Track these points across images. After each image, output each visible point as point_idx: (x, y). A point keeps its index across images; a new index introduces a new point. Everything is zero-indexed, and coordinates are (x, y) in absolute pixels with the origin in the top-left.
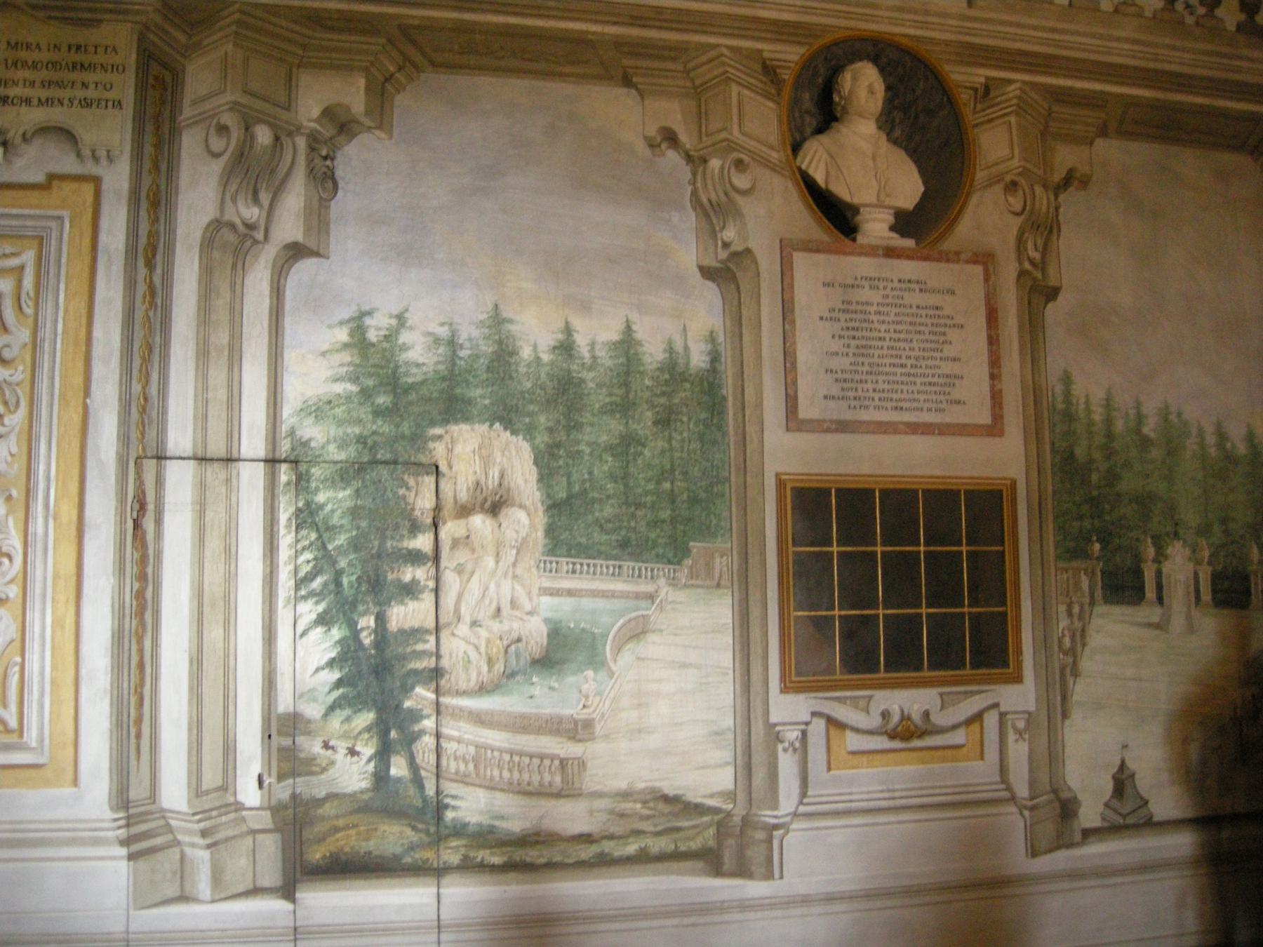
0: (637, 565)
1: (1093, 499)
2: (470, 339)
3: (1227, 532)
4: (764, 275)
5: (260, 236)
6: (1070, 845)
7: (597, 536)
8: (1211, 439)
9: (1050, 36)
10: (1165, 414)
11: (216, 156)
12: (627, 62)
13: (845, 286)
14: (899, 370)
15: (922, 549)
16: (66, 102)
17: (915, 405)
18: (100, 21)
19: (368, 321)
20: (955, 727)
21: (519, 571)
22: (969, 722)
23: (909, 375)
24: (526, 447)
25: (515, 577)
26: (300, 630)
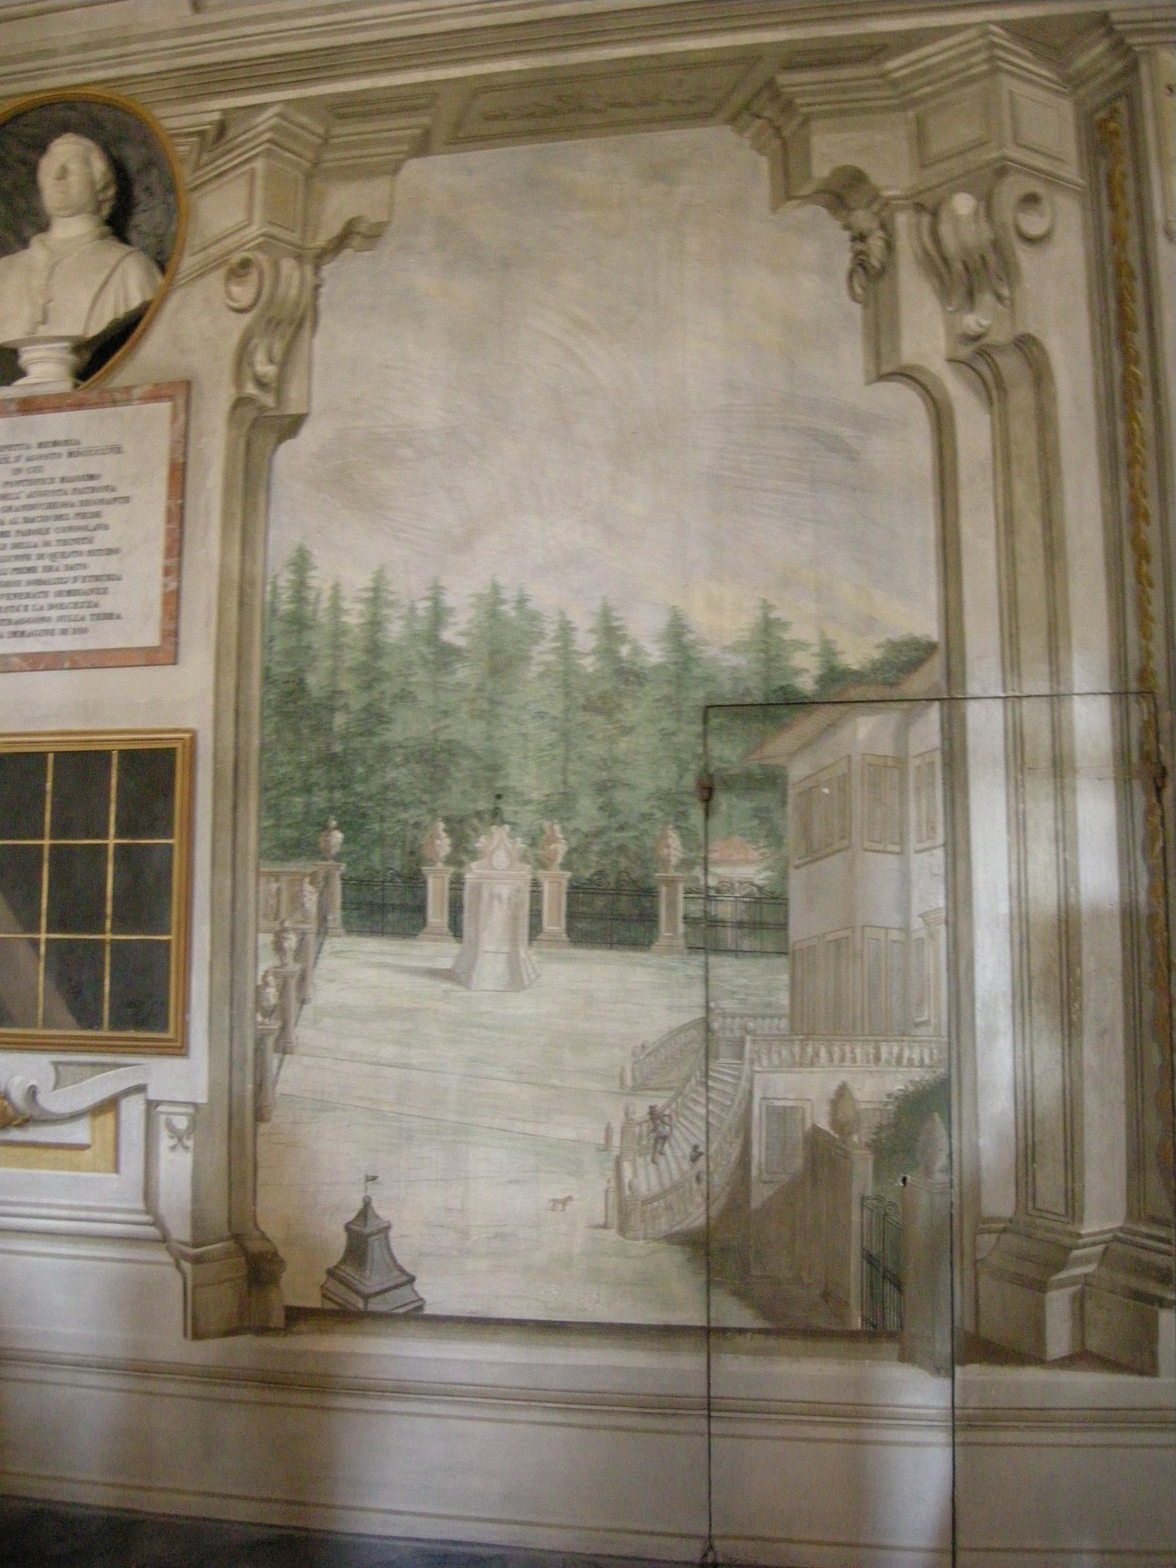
1: (333, 756)
3: (609, 809)
6: (263, 1330)
8: (586, 641)
10: (491, 603)
15: (47, 842)
20: (74, 1117)
23: (39, 582)
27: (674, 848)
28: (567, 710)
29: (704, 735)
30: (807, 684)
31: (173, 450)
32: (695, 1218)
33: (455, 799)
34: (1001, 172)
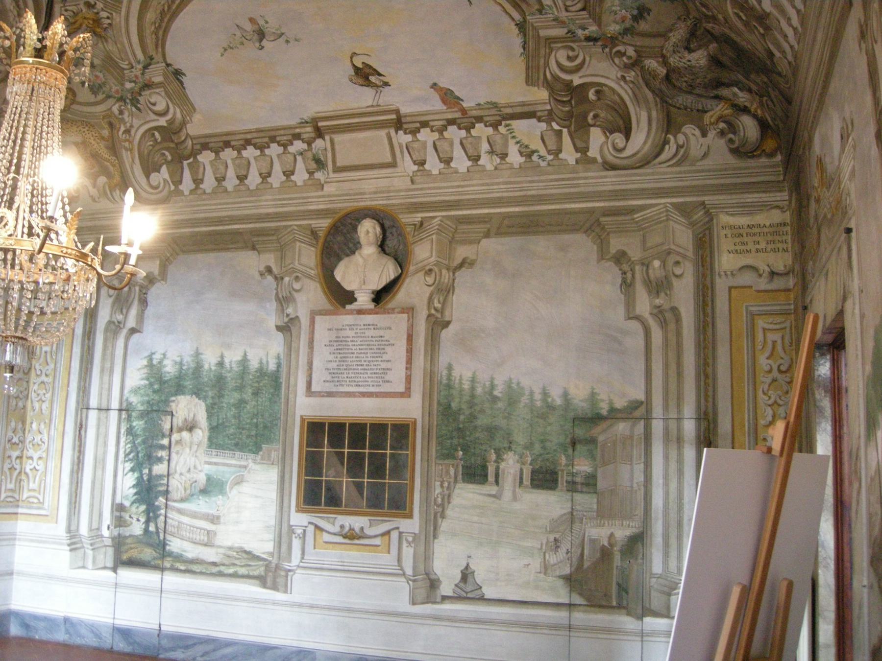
0: (241, 453)
2: (187, 362)
3: (544, 448)
4: (303, 327)
5: (122, 326)
6: (435, 603)
7: (227, 441)
8: (538, 396)
9: (457, 190)
10: (509, 384)
11: (110, 296)
12: (255, 239)
13: (337, 330)
14: (360, 367)
15: (367, 451)
17: (366, 383)
19: (154, 356)
20: (375, 536)
21: (198, 454)
22: (383, 535)
23: (365, 369)
24: (203, 404)
25: (196, 456)
26: (125, 472)
27: (563, 460)
28: (532, 417)
29: (574, 426)
30: (604, 412)
31: (408, 330)
32: (567, 571)
33: (497, 443)
34: (669, 253)
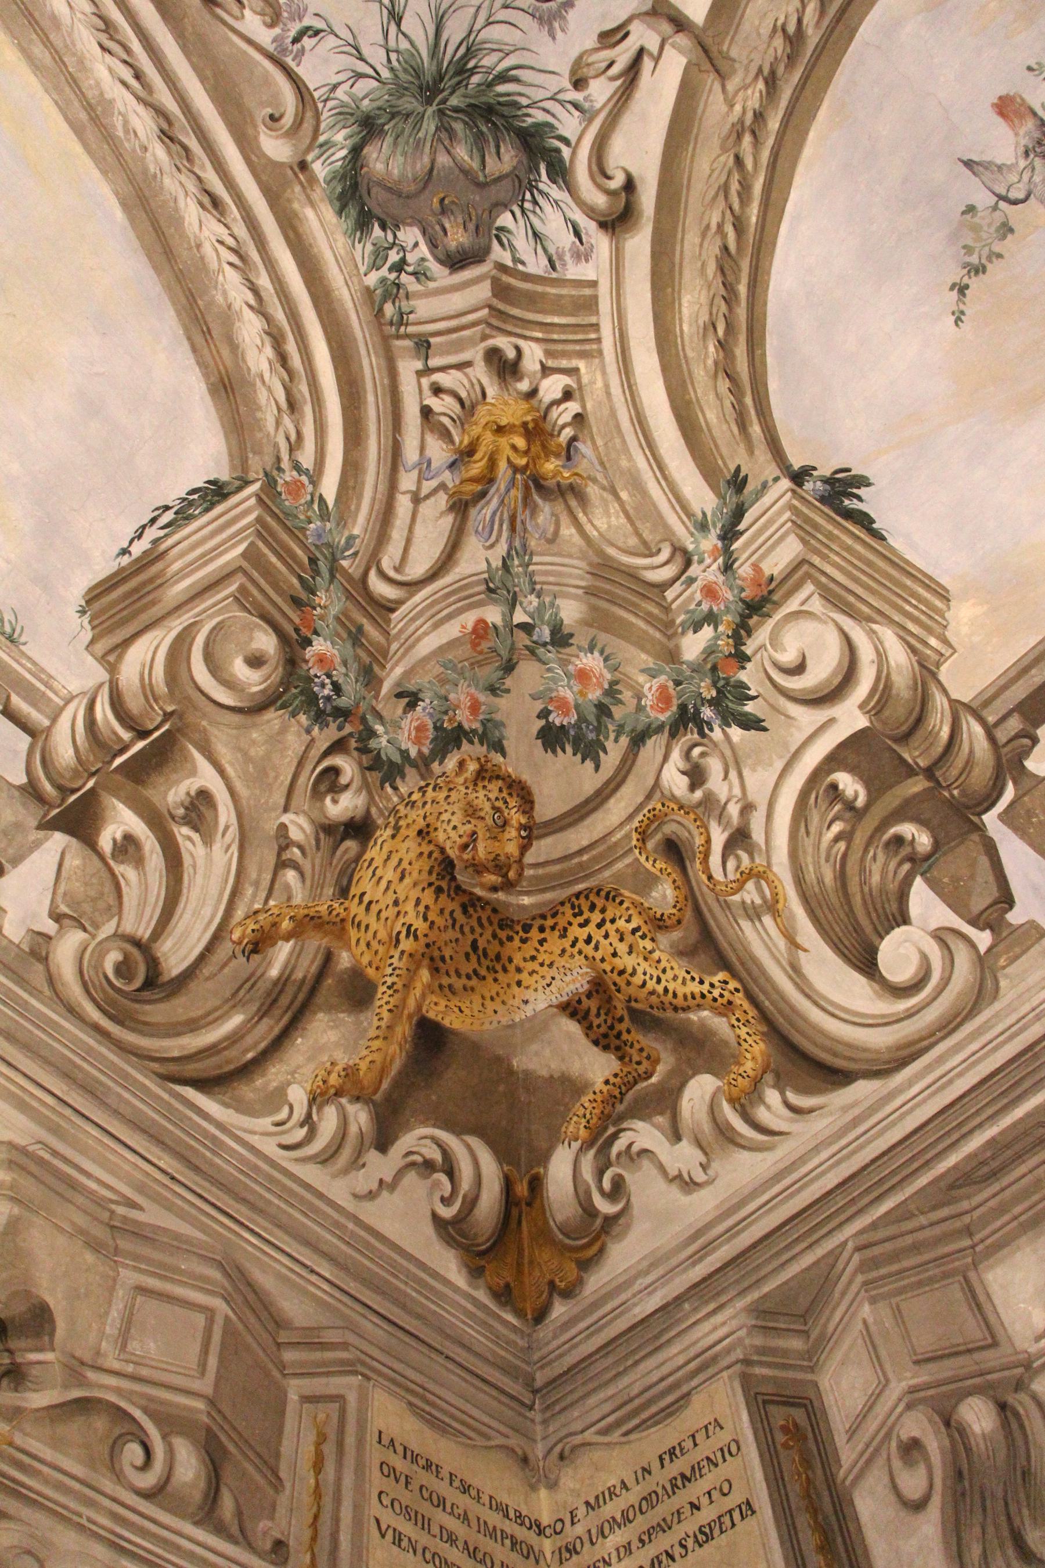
16: (677, 1551)
18: (688, 1394)
